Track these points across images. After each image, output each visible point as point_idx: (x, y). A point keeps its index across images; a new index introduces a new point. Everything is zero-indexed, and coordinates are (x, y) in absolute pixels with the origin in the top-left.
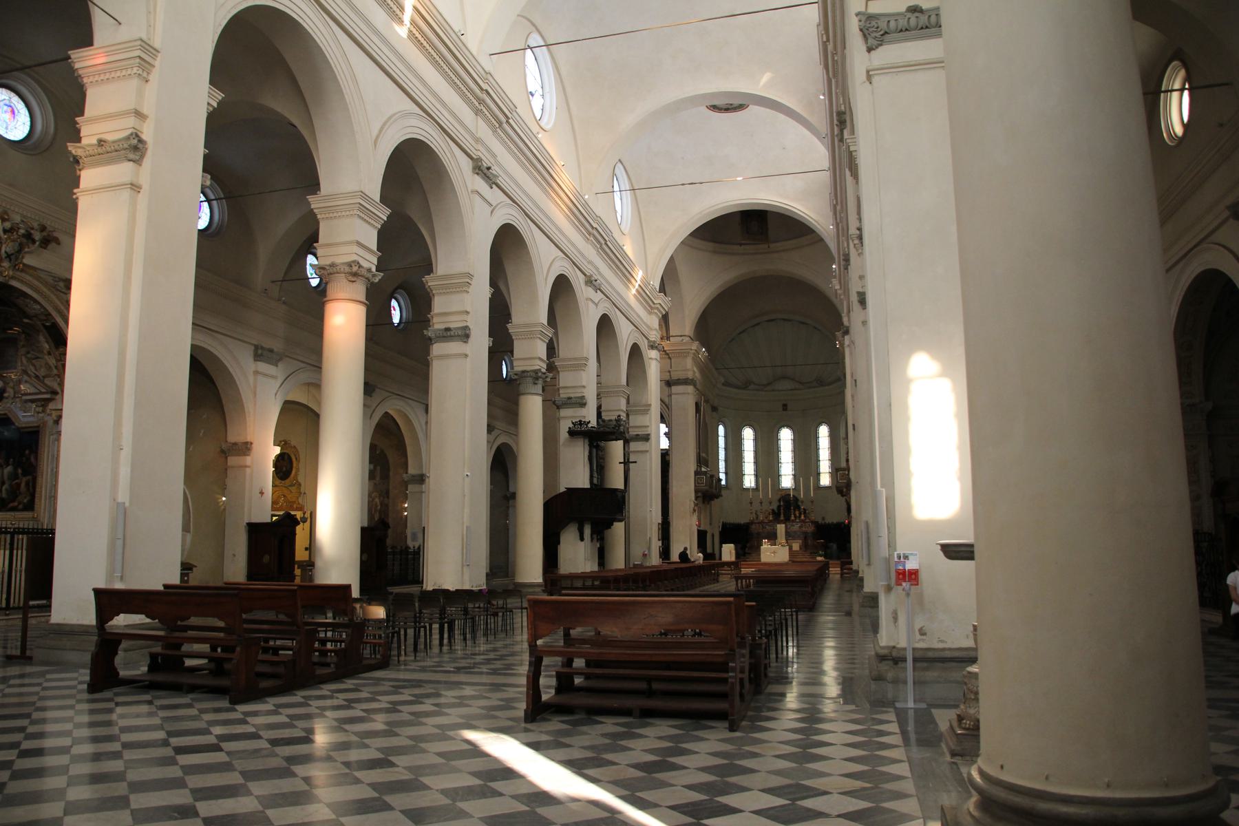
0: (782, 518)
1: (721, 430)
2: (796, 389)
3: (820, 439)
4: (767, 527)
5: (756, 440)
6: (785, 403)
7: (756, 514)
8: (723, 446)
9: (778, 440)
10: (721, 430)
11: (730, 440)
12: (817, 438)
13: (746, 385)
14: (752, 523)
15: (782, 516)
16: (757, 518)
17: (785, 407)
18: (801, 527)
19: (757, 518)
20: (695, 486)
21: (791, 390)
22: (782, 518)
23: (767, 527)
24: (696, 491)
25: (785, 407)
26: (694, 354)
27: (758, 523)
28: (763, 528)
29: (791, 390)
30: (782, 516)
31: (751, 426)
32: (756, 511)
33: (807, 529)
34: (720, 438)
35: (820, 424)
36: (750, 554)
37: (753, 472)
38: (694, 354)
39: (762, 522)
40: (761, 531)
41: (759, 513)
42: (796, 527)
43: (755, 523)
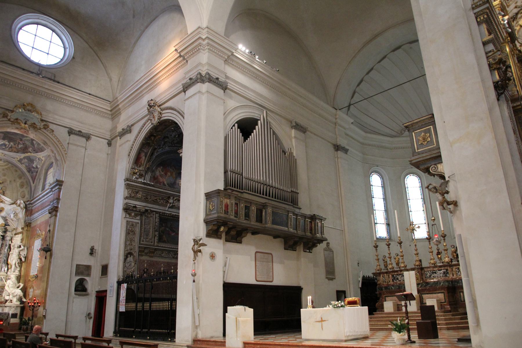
1: (376, 180)
7: (384, 260)
10: (376, 180)
11: (388, 189)
14: (377, 274)
16: (386, 266)
18: (446, 274)
19: (386, 266)
20: (207, 215)
24: (207, 222)
26: (208, 44)
27: (386, 273)
28: (394, 279)
33: (455, 276)
38: (208, 44)
40: (391, 283)
43: (383, 273)
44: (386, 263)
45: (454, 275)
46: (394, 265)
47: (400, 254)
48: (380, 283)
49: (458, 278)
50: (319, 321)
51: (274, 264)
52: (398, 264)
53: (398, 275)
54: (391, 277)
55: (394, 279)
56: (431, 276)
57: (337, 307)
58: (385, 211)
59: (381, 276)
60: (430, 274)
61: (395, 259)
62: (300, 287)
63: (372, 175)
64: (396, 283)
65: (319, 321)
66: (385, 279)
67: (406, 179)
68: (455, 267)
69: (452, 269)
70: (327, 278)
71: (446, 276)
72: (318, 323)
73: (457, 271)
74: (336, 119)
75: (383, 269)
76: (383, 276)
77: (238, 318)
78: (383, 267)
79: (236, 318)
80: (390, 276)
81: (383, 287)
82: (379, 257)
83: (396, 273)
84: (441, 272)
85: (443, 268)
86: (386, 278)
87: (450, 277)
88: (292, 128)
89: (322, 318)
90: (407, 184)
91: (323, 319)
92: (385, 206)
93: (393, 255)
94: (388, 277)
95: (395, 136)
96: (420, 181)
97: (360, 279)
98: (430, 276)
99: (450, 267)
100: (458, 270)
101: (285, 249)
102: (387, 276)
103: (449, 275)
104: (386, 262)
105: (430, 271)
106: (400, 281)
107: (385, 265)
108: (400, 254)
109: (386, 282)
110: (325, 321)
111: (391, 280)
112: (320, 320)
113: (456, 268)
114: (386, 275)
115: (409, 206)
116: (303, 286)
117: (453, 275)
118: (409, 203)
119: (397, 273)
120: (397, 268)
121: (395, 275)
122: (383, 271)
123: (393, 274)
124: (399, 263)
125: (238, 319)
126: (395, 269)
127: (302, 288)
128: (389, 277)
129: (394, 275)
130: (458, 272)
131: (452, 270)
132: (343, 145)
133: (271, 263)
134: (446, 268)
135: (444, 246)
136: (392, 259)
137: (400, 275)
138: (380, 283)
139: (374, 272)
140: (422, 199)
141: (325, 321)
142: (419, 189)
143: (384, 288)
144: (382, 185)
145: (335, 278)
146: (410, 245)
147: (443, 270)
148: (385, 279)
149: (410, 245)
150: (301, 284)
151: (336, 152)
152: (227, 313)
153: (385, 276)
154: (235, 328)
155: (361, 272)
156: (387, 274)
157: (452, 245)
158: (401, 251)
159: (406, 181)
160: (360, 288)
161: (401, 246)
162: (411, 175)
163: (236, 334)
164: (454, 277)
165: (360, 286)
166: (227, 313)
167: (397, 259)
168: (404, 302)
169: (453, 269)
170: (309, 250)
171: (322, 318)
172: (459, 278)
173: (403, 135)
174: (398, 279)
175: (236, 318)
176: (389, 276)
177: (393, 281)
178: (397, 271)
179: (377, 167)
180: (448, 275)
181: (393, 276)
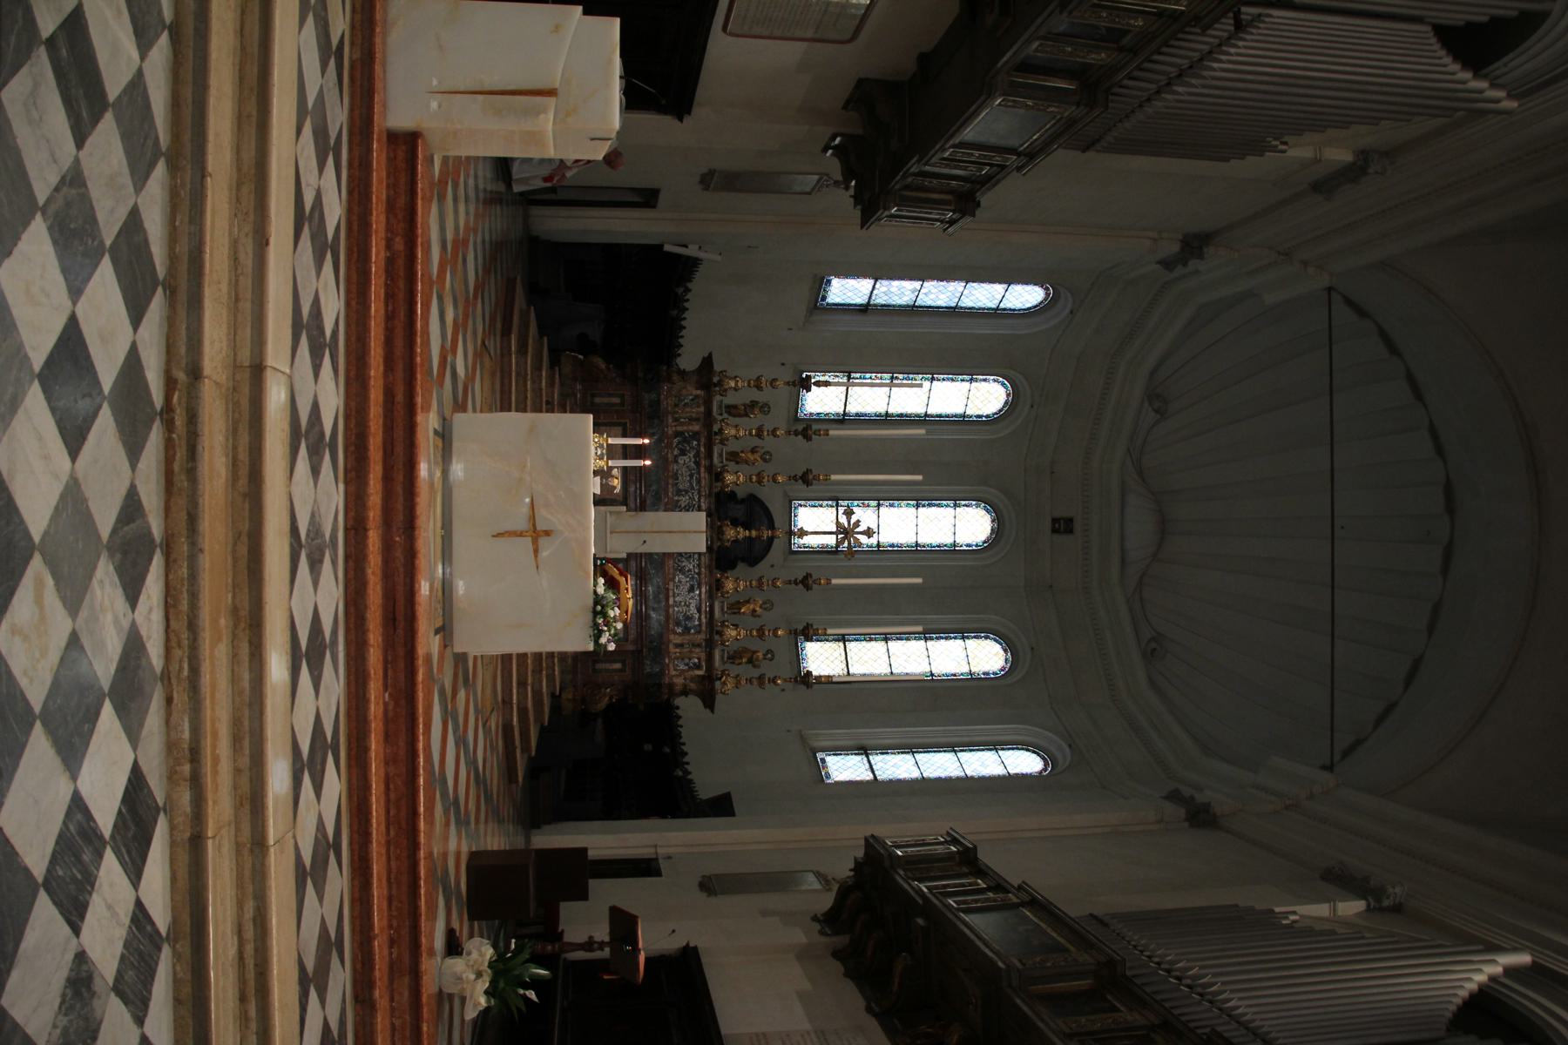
0: (730, 533)
1: (1026, 296)
2: (1123, 561)
3: (960, 642)
4: (687, 460)
5: (962, 422)
6: (1078, 526)
7: (753, 404)
8: (967, 302)
9: (956, 499)
10: (1026, 296)
12: (963, 632)
13: (1157, 399)
15: (743, 533)
16: (732, 410)
17: (1063, 526)
21: (1123, 550)
22: (730, 533)
23: (687, 460)
25: (1063, 526)
27: (709, 413)
28: (685, 439)
29: (1123, 550)
30: (743, 533)
31: (1011, 407)
32: (765, 408)
33: (672, 648)
34: (999, 288)
35: (1009, 644)
36: (555, 362)
37: (853, 408)
39: (711, 436)
41: (755, 420)
42: (687, 600)
43: (708, 403)
44: (742, 412)
45: (678, 650)
46: (733, 446)
47: (769, 469)
48: (674, 383)
49: (667, 661)
50: (533, 518)
51: (805, 44)
52: (734, 457)
53: (697, 455)
54: (691, 428)
55: (685, 440)
56: (683, 574)
57: (596, 625)
58: (914, 306)
59: (699, 392)
60: (690, 570)
61: (753, 451)
62: (689, 112)
63: (1047, 289)
64: (669, 446)
65: (533, 518)
66: (686, 405)
67: (1001, 379)
68: (703, 656)
69: (699, 645)
70: (711, 173)
71: (678, 624)
72: (525, 510)
73: (690, 659)
74: (1305, 263)
75: (722, 401)
76: (697, 397)
77: (551, 101)
78: (730, 399)
79: (551, 93)
80: (696, 427)
81: (659, 395)
82: (768, 390)
83: (702, 449)
84: (693, 610)
85: (703, 616)
86: (687, 410)
87: (672, 637)
88: (1363, 152)
89: (547, 533)
90: (985, 380)
91: (542, 541)
92: (930, 307)
93: (768, 443)
94: (694, 415)
95: (1153, 373)
96: (984, 419)
97: (692, 251)
98: (682, 570)
99: (706, 640)
100: (695, 664)
101: (861, 83)
102: (697, 413)
103: (679, 634)
104: (747, 415)
105: (699, 574)
106: (676, 462)
107: (735, 407)
108: (769, 469)
109: (676, 405)
110: (536, 551)
111: (680, 429)
112: (541, 526)
113: (699, 659)
114: (702, 409)
115: (911, 376)
116: (687, 119)
117: (681, 646)
118: (921, 376)
119: (702, 455)
120: (721, 455)
121: (699, 445)
122: (718, 398)
123: (703, 440)
124: (737, 463)
125: (537, 112)
126: (716, 450)
127: (681, 120)
128: (691, 419)
129: (699, 441)
130: (687, 665)
131: (693, 645)
132: (1194, 264)
133: (809, 34)
134: (704, 664)
135: (775, 630)
136: (756, 442)
137: (698, 464)
138: (674, 383)
139: (717, 367)
140: (926, 415)
141: (536, 551)
142: (960, 411)
143: (654, 396)
144: (1005, 309)
145: (707, 188)
146: (783, 364)
147: (697, 616)
148: (686, 405)
149: (783, 364)
150: (701, 112)
151: (1180, 237)
152: (585, 13)
153: (699, 406)
154: (492, 82)
155: (718, 258)
156: (702, 415)
157: (773, 655)
158: (780, 479)
159: (995, 381)
160: (661, 246)
161: (796, 480)
162: (1010, 399)
163: (462, 88)
164: (671, 646)
165: (667, 248)
166: (585, 13)
167: (751, 457)
168: (607, 939)
169: (698, 650)
170: (835, 148)
171: (547, 533)
172: (668, 665)
173: (1146, 404)
174: (683, 453)
175: (551, 93)
176: (697, 420)
177: (678, 434)
178: (709, 455)
179: (1067, 311)
180: (679, 630)
181: (695, 435)
